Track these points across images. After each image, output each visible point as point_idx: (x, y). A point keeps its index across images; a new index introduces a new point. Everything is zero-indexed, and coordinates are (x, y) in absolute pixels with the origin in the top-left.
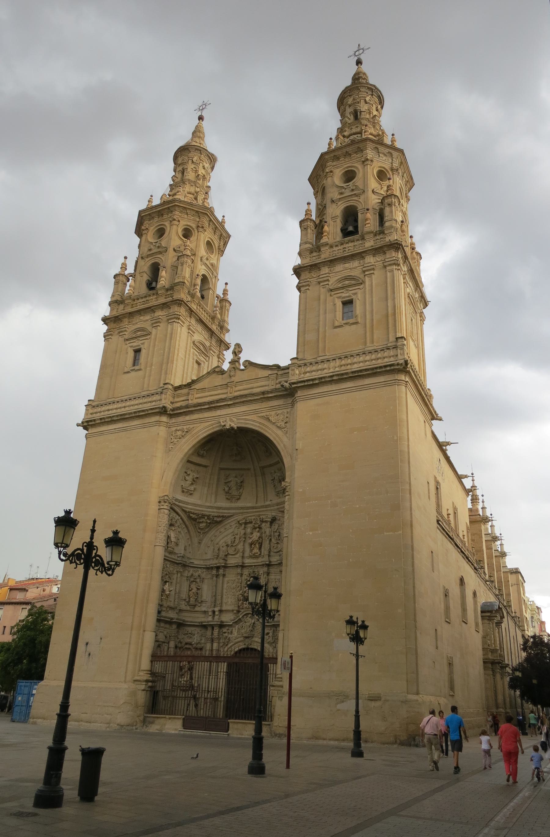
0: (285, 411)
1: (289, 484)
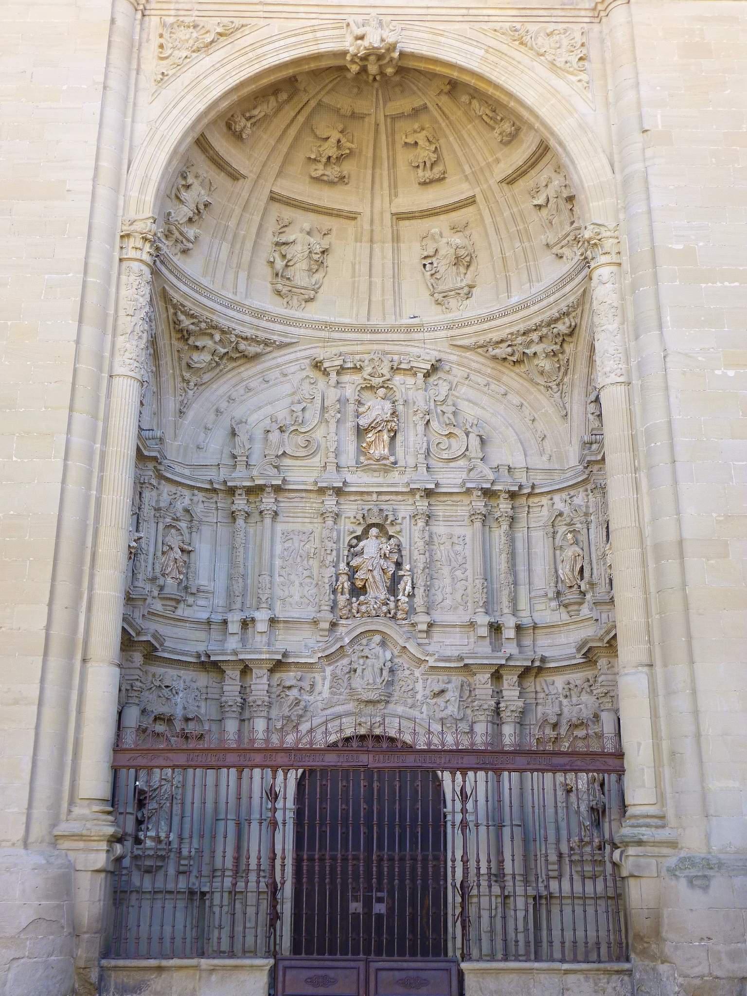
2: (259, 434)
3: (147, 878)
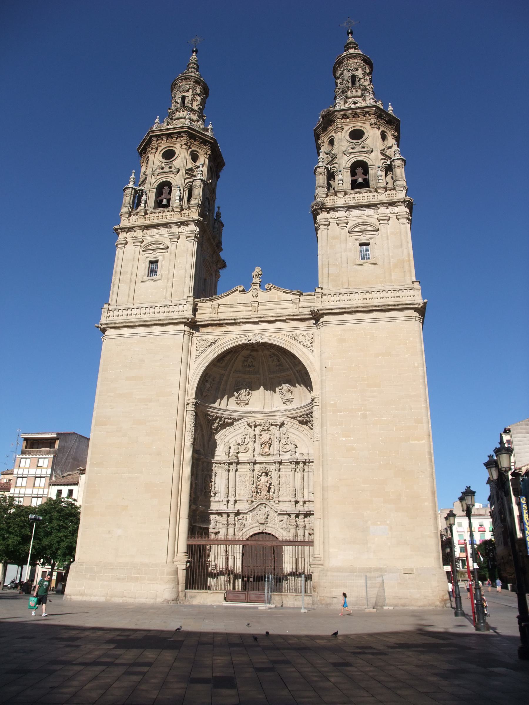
0: (311, 332)
1: (317, 396)
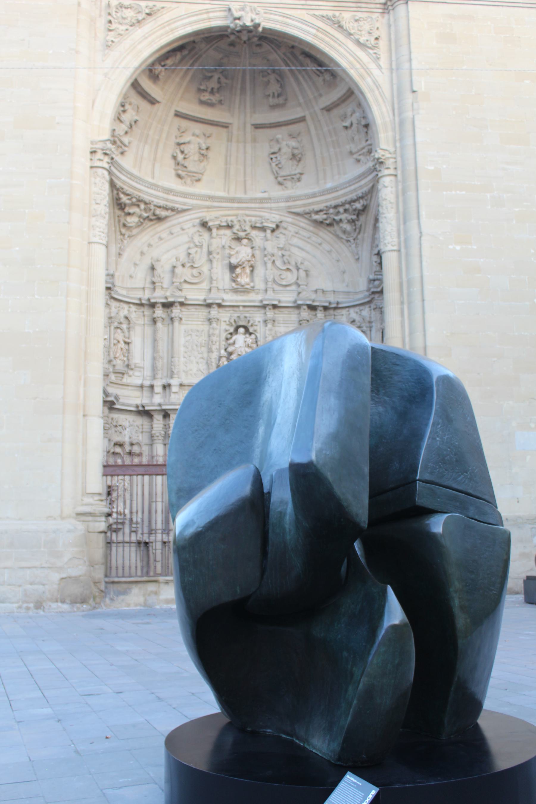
1: (389, 156)
2: (168, 268)
3: (114, 535)
